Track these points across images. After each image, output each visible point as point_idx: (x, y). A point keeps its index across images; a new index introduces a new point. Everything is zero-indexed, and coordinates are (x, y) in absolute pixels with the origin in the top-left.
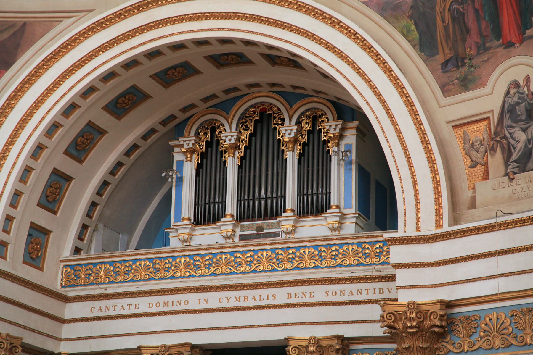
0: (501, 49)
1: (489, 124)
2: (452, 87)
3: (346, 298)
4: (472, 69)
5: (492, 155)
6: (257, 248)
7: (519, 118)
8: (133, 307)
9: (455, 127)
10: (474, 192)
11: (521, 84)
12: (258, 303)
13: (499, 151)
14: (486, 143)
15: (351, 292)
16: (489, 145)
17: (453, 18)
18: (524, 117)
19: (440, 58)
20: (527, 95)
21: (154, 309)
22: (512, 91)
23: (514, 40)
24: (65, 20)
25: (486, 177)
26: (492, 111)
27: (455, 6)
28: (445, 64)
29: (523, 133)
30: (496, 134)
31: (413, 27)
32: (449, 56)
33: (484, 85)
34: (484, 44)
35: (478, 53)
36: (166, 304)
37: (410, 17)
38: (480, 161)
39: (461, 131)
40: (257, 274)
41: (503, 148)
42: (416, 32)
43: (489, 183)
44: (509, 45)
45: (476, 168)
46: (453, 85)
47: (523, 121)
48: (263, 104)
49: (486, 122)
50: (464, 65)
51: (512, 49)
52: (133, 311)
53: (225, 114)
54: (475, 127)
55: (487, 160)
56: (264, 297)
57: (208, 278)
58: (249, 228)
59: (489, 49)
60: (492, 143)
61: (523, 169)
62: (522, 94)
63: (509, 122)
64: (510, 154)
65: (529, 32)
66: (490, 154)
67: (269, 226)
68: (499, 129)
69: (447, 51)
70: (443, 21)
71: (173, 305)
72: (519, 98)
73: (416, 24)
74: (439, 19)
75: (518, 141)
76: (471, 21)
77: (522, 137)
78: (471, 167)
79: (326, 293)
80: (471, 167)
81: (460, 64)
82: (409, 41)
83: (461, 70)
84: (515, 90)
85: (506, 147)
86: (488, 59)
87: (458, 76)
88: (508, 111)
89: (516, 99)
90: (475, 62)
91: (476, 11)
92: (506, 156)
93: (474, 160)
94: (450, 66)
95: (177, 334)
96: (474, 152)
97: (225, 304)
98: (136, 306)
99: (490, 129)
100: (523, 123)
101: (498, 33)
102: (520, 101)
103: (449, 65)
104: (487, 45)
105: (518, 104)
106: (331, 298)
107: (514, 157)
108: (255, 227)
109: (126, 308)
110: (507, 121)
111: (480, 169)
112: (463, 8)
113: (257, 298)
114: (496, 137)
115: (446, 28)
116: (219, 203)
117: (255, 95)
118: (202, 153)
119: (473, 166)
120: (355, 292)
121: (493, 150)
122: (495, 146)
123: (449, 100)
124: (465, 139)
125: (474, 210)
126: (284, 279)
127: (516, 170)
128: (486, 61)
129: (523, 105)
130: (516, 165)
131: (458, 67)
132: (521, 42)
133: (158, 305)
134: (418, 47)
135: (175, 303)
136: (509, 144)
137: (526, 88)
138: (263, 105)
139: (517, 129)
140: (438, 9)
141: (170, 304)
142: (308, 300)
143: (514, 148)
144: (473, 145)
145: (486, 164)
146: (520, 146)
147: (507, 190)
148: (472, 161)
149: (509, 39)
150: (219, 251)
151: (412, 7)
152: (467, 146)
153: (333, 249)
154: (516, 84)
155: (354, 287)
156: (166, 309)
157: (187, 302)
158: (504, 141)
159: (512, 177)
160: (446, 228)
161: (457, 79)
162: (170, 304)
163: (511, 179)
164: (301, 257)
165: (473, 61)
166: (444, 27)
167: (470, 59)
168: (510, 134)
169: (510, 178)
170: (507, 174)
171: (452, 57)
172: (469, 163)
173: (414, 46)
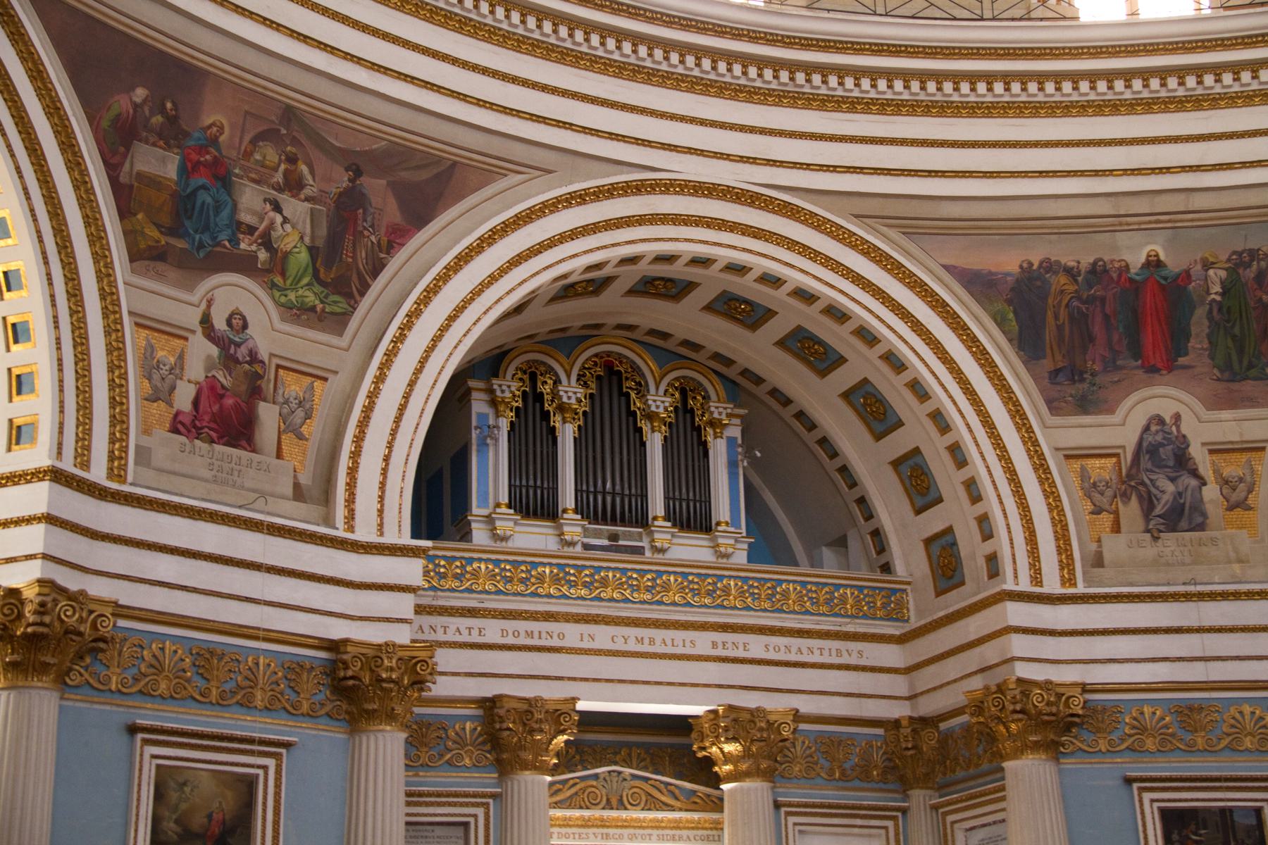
0: (1140, 372)
1: (1119, 463)
2: (1064, 404)
3: (793, 657)
4: (1095, 388)
5: (1125, 503)
6: (663, 568)
7: (1164, 463)
8: (475, 632)
9: (1067, 457)
10: (1100, 546)
11: (1168, 420)
12: (670, 650)
13: (1134, 498)
14: (1114, 486)
15: (800, 650)
16: (1119, 489)
17: (1071, 317)
18: (1171, 463)
19: (1047, 364)
20: (1177, 437)
21: (510, 640)
22: (1154, 428)
23: (1159, 365)
24: (513, 174)
25: (1116, 528)
26: (1123, 447)
27: (1075, 303)
28: (1056, 373)
29: (1169, 483)
30: (1128, 475)
31: (1011, 316)
32: (1060, 365)
33: (1111, 411)
34: (1114, 361)
35: (1105, 370)
36: (530, 634)
37: (1009, 302)
38: (1107, 507)
39: (1077, 465)
40: (663, 607)
41: (1140, 498)
42: (1014, 323)
43: (1122, 539)
44: (1152, 370)
45: (1101, 516)
46: (1066, 402)
47: (1169, 467)
48: (609, 354)
49: (1114, 460)
50: (1082, 380)
51: (1156, 376)
52: (475, 638)
53: (563, 359)
54: (1098, 462)
55: (1117, 508)
56: (679, 642)
57: (588, 603)
58: (597, 535)
59: (1121, 368)
60: (1123, 487)
61: (1173, 528)
62: (1169, 434)
63: (1149, 466)
64: (1151, 507)
65: (1182, 361)
66: (1121, 500)
67: (629, 536)
68: (1134, 471)
69: (1058, 357)
70: (1056, 317)
71: (540, 638)
72: (1164, 438)
73: (1015, 313)
74: (1050, 314)
75: (1163, 492)
76: (1097, 329)
77: (1170, 488)
78: (1092, 513)
79: (766, 646)
80: (1092, 513)
81: (1076, 378)
82: (1004, 332)
83: (1077, 385)
84: (1159, 428)
85: (1145, 495)
86: (1119, 381)
87: (1073, 392)
88: (1148, 452)
89: (1159, 438)
90: (1098, 380)
91: (1106, 317)
92: (1145, 507)
93: (1097, 504)
94: (1061, 378)
95: (543, 681)
96: (1097, 495)
97: (620, 646)
98: (480, 632)
99: (1120, 469)
100: (1169, 470)
101: (1136, 350)
102: (1165, 442)
103: (1061, 375)
104: (1119, 363)
105: (1161, 445)
106: (772, 655)
107: (1159, 510)
108: (606, 534)
109: (465, 632)
110: (1145, 462)
111: (1106, 519)
112: (1087, 309)
113: (669, 642)
114: (1131, 480)
115: (1060, 328)
116: (636, 496)
117: (605, 340)
118: (585, 412)
119: (1097, 511)
120: (805, 651)
121: (1125, 497)
122: (1128, 492)
123: (1058, 420)
124: (1084, 475)
125: (1101, 570)
126: (683, 618)
127: (1162, 527)
128: (1116, 382)
129: (1170, 447)
130: (1162, 521)
131: (1073, 381)
132: (1170, 369)
133: (516, 634)
134: (1015, 342)
135: (544, 635)
136: (1149, 493)
137: (1174, 429)
138: (608, 356)
139: (1161, 476)
140: (1050, 301)
141: (536, 635)
142: (740, 653)
143: (1158, 500)
144: (1094, 485)
145: (1116, 513)
146: (1165, 498)
147: (1149, 551)
148: (1095, 505)
149: (1152, 363)
150: (605, 564)
151: (1012, 290)
152: (1086, 485)
153: (769, 585)
154: (1161, 421)
155: (795, 642)
156: (529, 642)
157: (561, 636)
158: (1141, 488)
159: (1156, 535)
160: (1081, 589)
161: (1071, 396)
162: (536, 635)
163: (1156, 539)
164: (666, 587)
165: (1096, 378)
166: (1058, 327)
167: (1092, 375)
168: (1151, 480)
169: (1153, 536)
170: (1148, 531)
171: (1065, 367)
172: (1090, 507)
173: (1010, 341)
